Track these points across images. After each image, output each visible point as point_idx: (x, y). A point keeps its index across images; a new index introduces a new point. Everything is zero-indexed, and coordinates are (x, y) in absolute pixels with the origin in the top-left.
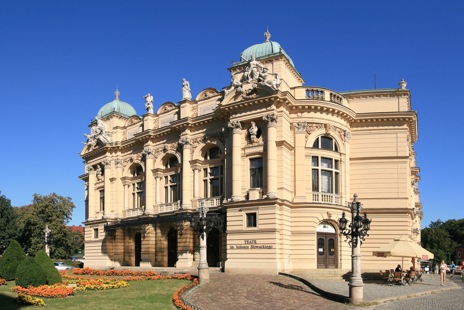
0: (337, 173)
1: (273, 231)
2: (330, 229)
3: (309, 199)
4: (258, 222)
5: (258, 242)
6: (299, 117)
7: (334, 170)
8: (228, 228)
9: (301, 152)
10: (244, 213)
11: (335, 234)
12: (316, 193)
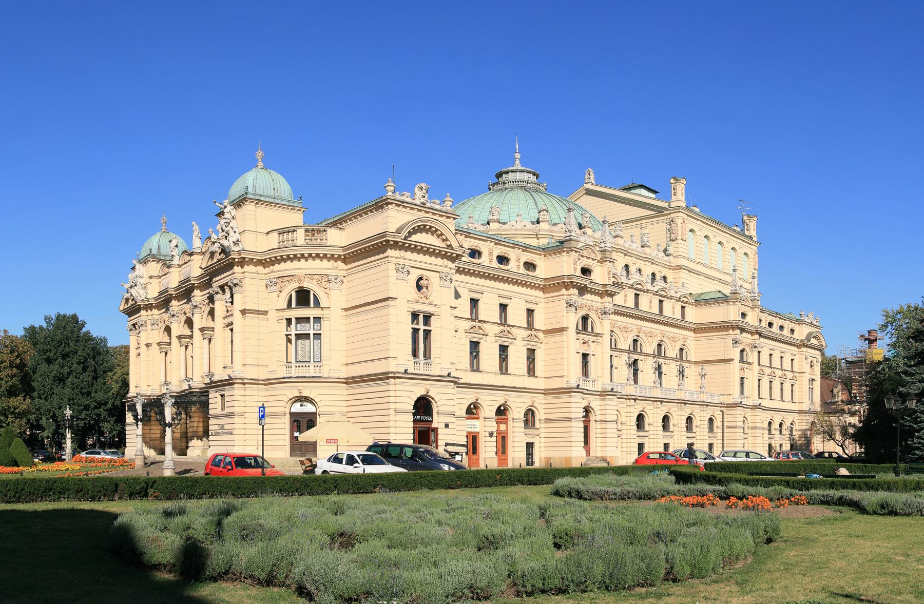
0: (318, 336)
1: (231, 415)
2: (309, 408)
3: (282, 373)
4: (227, 404)
5: (226, 427)
6: (272, 272)
7: (312, 332)
8: (211, 412)
9: (273, 315)
10: (218, 395)
11: (314, 414)
12: (289, 365)
